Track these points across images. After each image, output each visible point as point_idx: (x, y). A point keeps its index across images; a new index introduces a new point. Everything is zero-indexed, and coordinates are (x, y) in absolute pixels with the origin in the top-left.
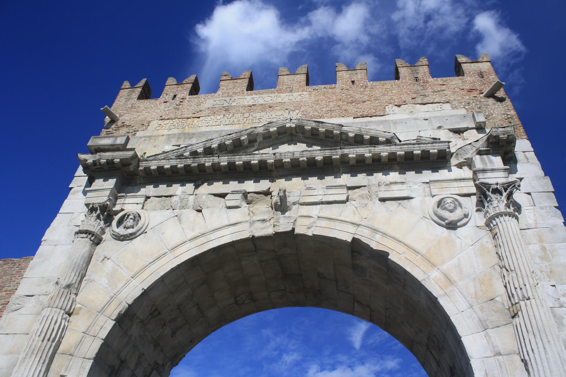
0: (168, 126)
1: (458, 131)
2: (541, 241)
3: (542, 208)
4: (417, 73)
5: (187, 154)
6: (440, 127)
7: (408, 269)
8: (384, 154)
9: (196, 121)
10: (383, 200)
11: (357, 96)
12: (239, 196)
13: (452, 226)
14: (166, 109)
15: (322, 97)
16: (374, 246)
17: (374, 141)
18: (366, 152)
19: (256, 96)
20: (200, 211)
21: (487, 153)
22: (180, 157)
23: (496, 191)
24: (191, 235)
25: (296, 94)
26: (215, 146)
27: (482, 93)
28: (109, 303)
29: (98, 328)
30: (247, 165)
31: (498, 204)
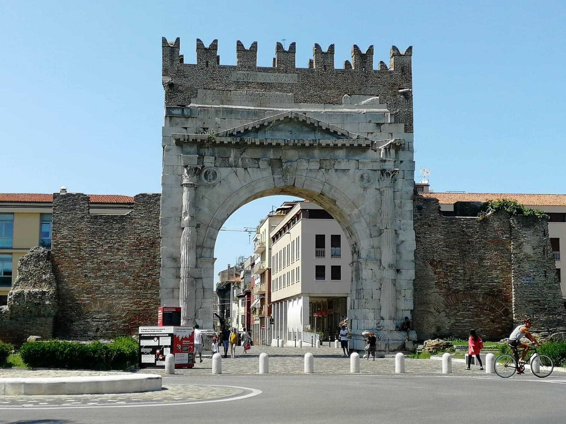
0: (211, 95)
1: (379, 125)
2: (401, 198)
3: (406, 180)
4: (366, 62)
5: (235, 133)
6: (370, 122)
7: (344, 209)
8: (339, 145)
9: (229, 94)
10: (336, 170)
11: (328, 83)
12: (266, 163)
13: (365, 189)
14: (205, 77)
15: (306, 81)
16: (330, 196)
17: (335, 133)
18: (331, 141)
19: (264, 73)
20: (246, 169)
21: (389, 149)
22: (231, 135)
23: (388, 174)
24: (244, 184)
25: (290, 75)
26: (250, 129)
27: (400, 89)
28: (213, 222)
29: (212, 234)
30: (270, 145)
31: (387, 181)
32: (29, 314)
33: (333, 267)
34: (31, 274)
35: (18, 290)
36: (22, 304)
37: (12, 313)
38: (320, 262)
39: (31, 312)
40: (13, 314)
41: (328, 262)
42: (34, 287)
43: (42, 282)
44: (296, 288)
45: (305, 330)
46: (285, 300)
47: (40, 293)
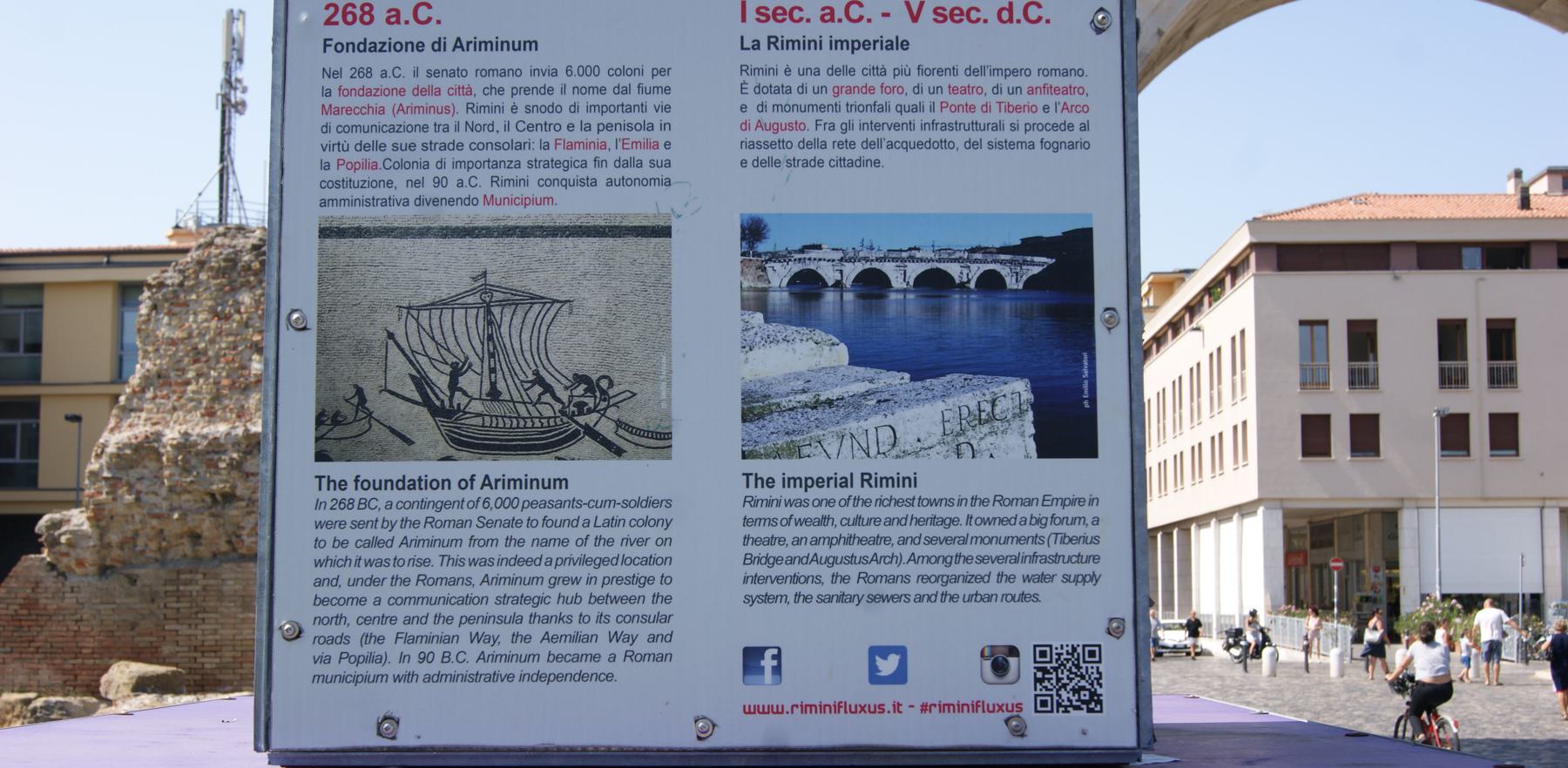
32: (186, 547)
33: (1355, 419)
34: (197, 355)
35: (134, 430)
36: (152, 499)
37: (105, 546)
38: (1315, 404)
39: (195, 537)
40: (109, 545)
41: (1341, 403)
42: (210, 414)
43: (246, 389)
44: (1242, 483)
45: (1274, 610)
46: (1184, 526)
47: (236, 444)
